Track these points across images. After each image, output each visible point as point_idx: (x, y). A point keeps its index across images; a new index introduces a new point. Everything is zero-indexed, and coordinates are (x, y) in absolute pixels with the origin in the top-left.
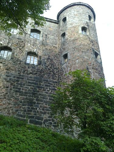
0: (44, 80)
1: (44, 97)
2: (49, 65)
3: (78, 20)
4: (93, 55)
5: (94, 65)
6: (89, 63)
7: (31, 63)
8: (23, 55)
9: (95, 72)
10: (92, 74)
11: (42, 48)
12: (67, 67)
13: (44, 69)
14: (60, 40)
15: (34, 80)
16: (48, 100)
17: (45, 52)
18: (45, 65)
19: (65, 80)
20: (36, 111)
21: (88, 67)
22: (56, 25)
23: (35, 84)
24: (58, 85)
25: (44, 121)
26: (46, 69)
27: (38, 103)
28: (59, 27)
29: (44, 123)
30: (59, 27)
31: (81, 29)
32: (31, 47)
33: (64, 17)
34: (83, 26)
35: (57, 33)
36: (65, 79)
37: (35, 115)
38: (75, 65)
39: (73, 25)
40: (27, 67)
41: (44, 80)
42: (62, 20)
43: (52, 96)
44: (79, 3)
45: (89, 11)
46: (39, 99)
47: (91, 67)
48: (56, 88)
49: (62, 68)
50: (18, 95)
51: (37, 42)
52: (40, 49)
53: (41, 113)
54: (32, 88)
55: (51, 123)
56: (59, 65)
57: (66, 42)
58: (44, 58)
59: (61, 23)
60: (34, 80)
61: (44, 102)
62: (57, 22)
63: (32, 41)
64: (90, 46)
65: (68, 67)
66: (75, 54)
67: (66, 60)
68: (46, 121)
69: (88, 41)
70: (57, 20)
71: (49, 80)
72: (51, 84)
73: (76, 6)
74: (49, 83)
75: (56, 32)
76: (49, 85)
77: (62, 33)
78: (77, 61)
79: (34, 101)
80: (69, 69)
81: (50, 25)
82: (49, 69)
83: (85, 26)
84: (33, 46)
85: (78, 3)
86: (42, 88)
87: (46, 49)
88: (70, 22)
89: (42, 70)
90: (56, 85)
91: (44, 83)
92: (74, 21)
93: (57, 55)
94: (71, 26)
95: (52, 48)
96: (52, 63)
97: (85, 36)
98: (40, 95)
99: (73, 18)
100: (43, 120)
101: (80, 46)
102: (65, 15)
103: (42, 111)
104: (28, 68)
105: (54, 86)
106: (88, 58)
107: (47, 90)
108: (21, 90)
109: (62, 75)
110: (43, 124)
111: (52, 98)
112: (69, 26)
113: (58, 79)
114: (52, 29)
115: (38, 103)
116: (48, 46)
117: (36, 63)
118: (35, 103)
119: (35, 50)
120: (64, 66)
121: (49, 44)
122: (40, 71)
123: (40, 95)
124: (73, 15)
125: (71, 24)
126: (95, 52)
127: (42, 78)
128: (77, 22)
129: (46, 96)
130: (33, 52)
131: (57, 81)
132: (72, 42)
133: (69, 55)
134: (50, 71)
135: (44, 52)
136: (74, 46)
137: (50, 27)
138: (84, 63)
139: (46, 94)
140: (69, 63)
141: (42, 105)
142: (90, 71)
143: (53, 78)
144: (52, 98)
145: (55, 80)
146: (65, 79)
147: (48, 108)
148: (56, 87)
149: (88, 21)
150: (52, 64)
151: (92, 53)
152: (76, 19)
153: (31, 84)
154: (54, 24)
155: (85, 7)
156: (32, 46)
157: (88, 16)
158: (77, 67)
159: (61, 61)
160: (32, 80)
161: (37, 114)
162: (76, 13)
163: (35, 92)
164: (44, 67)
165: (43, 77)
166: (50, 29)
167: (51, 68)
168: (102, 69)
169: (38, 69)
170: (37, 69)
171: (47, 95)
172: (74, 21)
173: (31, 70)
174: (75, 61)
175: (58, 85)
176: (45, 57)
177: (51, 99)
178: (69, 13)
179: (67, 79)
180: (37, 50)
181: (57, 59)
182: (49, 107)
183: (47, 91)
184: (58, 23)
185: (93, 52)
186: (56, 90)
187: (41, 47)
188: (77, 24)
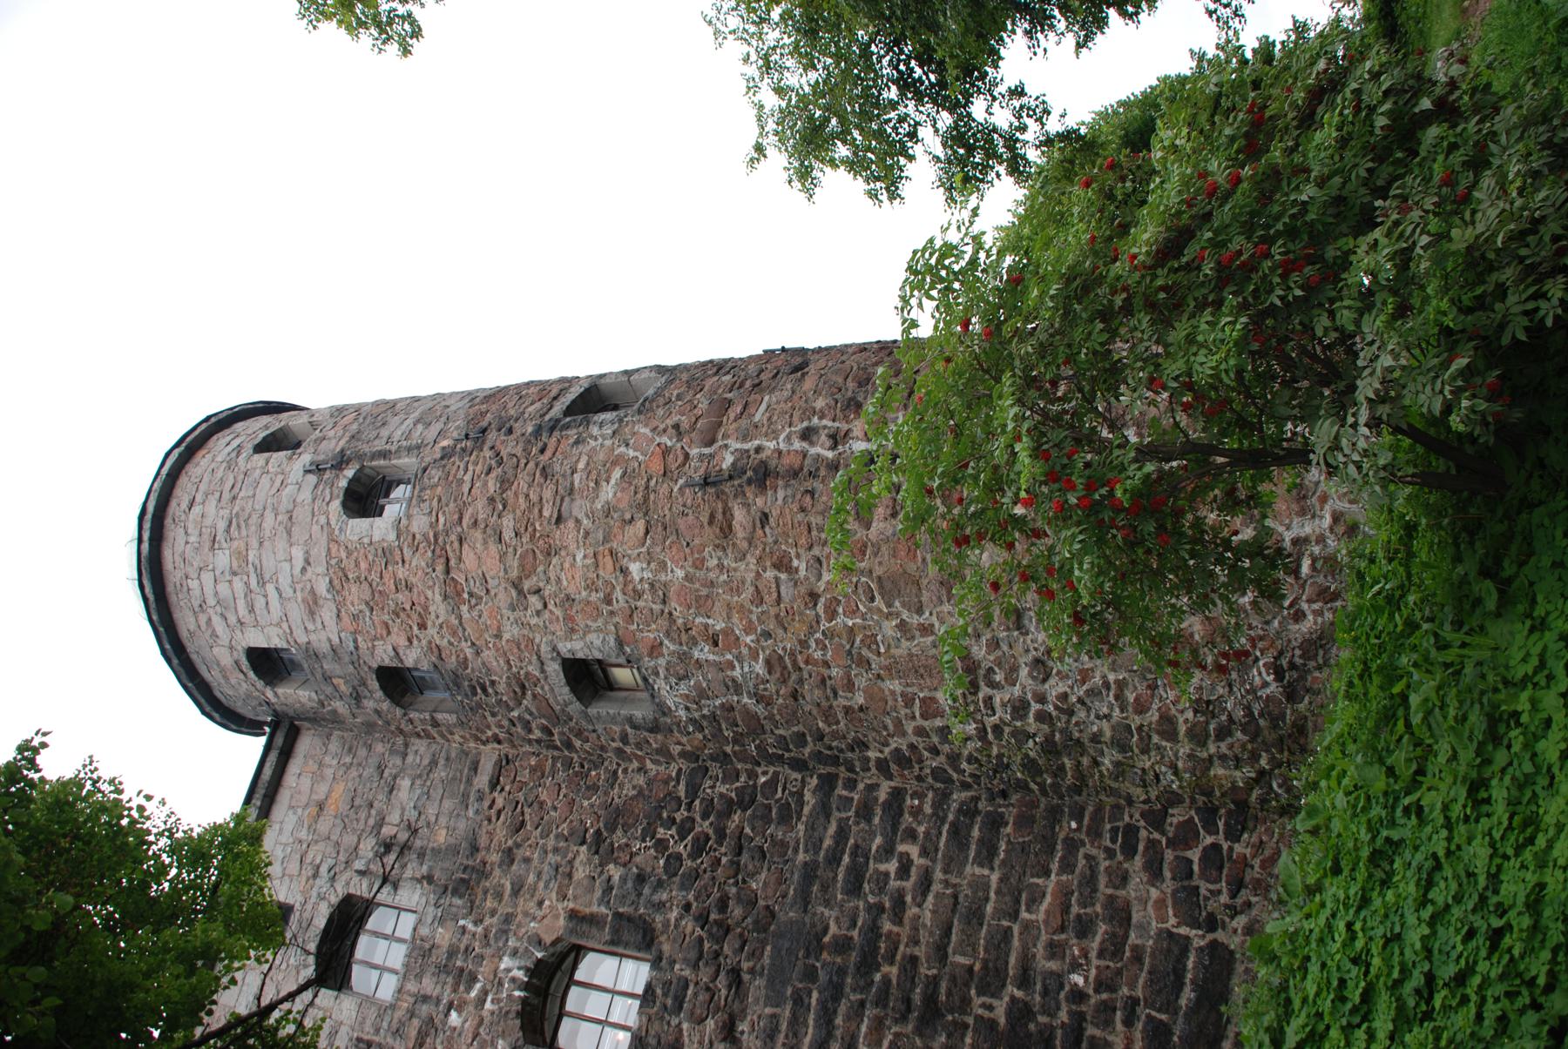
0: (804, 900)
1: (961, 909)
2: (661, 845)
3: (281, 544)
4: (595, 430)
5: (685, 425)
6: (656, 467)
7: (632, 1020)
9: (744, 422)
10: (758, 450)
11: (499, 896)
12: (683, 668)
13: (691, 897)
14: (439, 716)
15: (799, 1001)
16: (995, 878)
17: (539, 875)
18: (660, 884)
19: (811, 693)
20: (1104, 1002)
21: (697, 478)
22: (307, 743)
23: (835, 992)
24: (851, 769)
25: (1195, 924)
26: (696, 875)
27: (1024, 981)
28: (323, 720)
29: (1212, 924)
30: (323, 720)
31: (359, 527)
32: (481, 1001)
33: (245, 663)
34: (336, 504)
35: (379, 748)
36: (795, 695)
37: (1143, 1012)
38: (672, 594)
39: (322, 587)
41: (804, 900)
42: (269, 694)
43: (959, 835)
44: (147, 525)
45: (221, 445)
46: (985, 967)
47: (694, 452)
48: (882, 795)
49: (692, 721)
51: (444, 936)
52: (508, 919)
53: (1114, 947)
54: (878, 1026)
55: (1213, 857)
56: (664, 752)
57: (464, 663)
58: (591, 890)
59: (293, 695)
60: (799, 1001)
61: (1014, 916)
62: (279, 740)
63: (428, 985)
64: (519, 451)
65: (684, 657)
66: (571, 590)
67: (623, 675)
68: (1188, 903)
69: (469, 471)
70: (263, 740)
71: (801, 857)
72: (842, 834)
73: (167, 554)
74: (834, 859)
75: (362, 752)
76: (854, 854)
77: (376, 700)
78: (635, 568)
79: (1000, 1014)
80: (703, 652)
81: (304, 799)
82: (699, 848)
83: (343, 483)
84: (473, 979)
85: (146, 536)
86: (873, 930)
87: (509, 856)
88: (297, 613)
89: (703, 920)
90: (851, 784)
91: (827, 904)
92: (285, 582)
93: (568, 764)
94: (327, 613)
95: (500, 802)
96: (640, 808)
97: (427, 494)
98: (941, 952)
99: (262, 582)
100: (1183, 930)
101: (508, 535)
102: (226, 660)
103: (1098, 938)
105: (865, 812)
106: (617, 473)
107: (894, 884)
109: (756, 727)
110: (1220, 935)
111: (976, 833)
112: (325, 632)
113: (799, 765)
114: (340, 788)
115: (1024, 981)
116: (483, 841)
117: (634, 974)
118: (1020, 1012)
119: (506, 962)
120: (673, 696)
121: (462, 825)
122: (710, 934)
123: (941, 952)
124: (238, 585)
125: (312, 605)
126: (569, 411)
127: (782, 917)
128: (298, 554)
129: (955, 897)
130: (526, 987)
131: (815, 781)
132: (464, 608)
133: (576, 647)
134: (721, 835)
135: (531, 878)
136: (504, 596)
137: (321, 806)
138: (661, 508)
139: (936, 887)
140: (655, 649)
141: (1044, 937)
142: (729, 460)
143: (787, 815)
144: (976, 833)
145: (808, 796)
146: (795, 695)
147: (1073, 880)
148: (873, 788)
149: (305, 458)
150: (654, 819)
151: (572, 432)
152: (269, 565)
153: (830, 1035)
154: (294, 767)
155: (183, 480)
156: (469, 989)
157: (260, 459)
158: (688, 578)
159: (630, 720)
160: (796, 1022)
161: (1125, 991)
162: (223, 559)
163: (917, 997)
164: (673, 894)
165: (773, 915)
166: (330, 810)
168: (719, 367)
169: (693, 955)
170: (695, 967)
171: (946, 883)
172: (285, 582)
173: (702, 1021)
174: (638, 595)
175: (851, 769)
176: (580, 873)
177: (981, 841)
178: (216, 620)
179: (801, 681)
180: (514, 953)
181: (611, 761)
182: (1055, 866)
183: (908, 885)
184: (293, 734)
185: (567, 427)
186: (897, 795)
187: (490, 903)
188: (319, 552)
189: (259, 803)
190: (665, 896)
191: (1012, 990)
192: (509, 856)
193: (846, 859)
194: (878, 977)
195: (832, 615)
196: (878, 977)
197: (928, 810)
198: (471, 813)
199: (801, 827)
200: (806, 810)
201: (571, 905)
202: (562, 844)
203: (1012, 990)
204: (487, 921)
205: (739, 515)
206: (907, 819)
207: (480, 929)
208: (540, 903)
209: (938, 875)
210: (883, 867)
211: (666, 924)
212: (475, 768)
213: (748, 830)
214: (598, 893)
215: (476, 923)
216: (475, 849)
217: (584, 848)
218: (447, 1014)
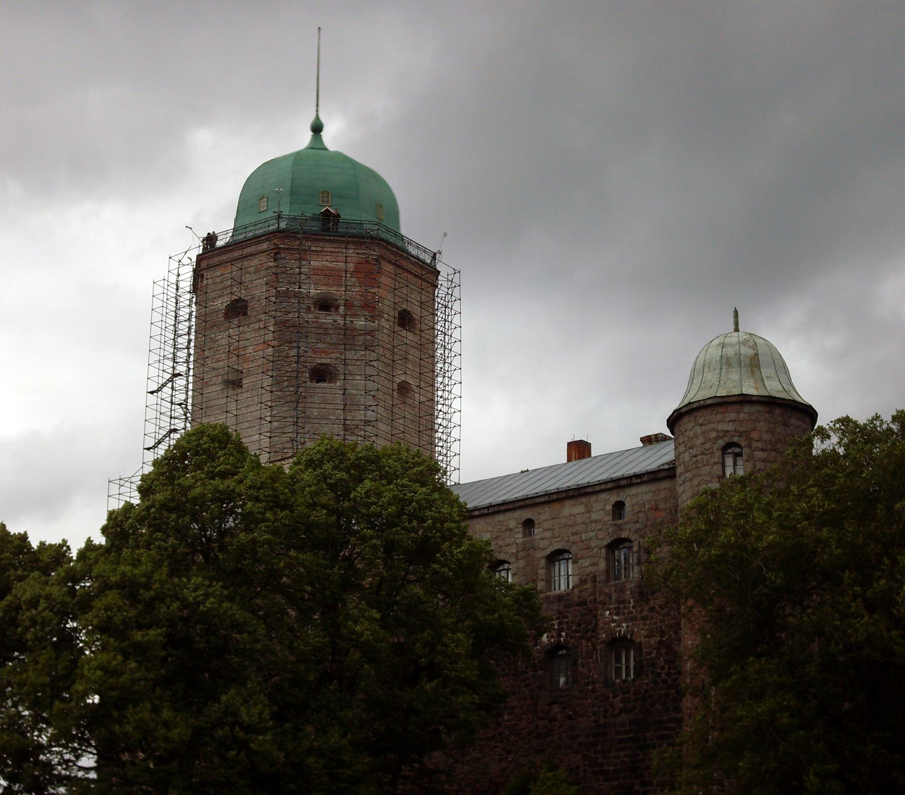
17: (650, 625)
40: (611, 695)
50: (601, 783)
82: (665, 682)
87: (652, 609)
89: (646, 691)
108: (606, 768)
116: (656, 596)
135: (648, 622)
167: (668, 674)
180: (627, 626)
189: (650, 479)
190: (650, 676)
191: (642, 789)
192: (652, 609)
193: (666, 732)
194: (639, 752)
196: (639, 752)
199: (673, 715)
200: (678, 715)
201: (643, 642)
202: (659, 629)
203: (642, 789)
204: (634, 611)
207: (631, 609)
208: (642, 629)
211: (643, 680)
213: (671, 697)
214: (648, 650)
215: (633, 607)
216: (653, 593)
217: (659, 638)
218: (608, 610)
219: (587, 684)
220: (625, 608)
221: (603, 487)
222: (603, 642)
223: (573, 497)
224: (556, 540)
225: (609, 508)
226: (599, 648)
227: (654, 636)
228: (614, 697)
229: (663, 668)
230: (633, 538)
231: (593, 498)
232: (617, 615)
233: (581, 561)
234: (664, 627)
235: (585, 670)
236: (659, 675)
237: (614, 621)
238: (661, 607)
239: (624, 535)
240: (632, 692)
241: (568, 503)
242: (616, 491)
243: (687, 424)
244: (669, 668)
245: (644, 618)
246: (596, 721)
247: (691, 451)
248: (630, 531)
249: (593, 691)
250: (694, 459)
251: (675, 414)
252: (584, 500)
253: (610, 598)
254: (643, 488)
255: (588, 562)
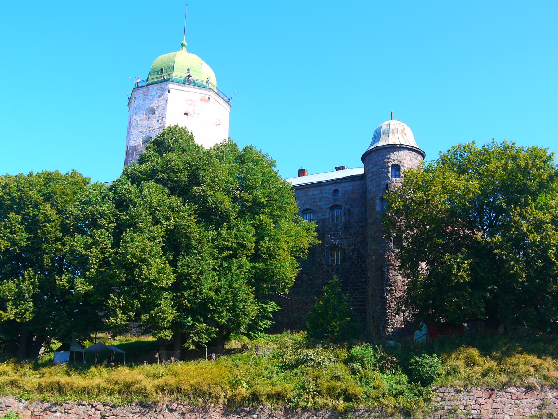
8: (324, 254)
17: (349, 241)
40: (331, 271)
82: (356, 265)
87: (351, 235)
101: (377, 234)
104: (332, 271)
106: (383, 252)
107: (354, 294)
111: (361, 303)
135: (348, 240)
139: (354, 300)
142: (384, 269)
144: (361, 303)
167: (358, 262)
176: (350, 248)
180: (339, 241)
195: (371, 286)
197: (364, 297)
198: (356, 224)
205: (378, 272)
206: (362, 294)
208: (346, 243)
209: (356, 300)
210: (356, 293)
211: (346, 264)
212: (362, 221)
214: (348, 252)
219: (320, 266)
220: (338, 234)
221: (329, 183)
222: (328, 248)
223: (315, 187)
224: (306, 204)
225: (331, 192)
226: (325, 250)
227: (351, 246)
228: (332, 271)
229: (355, 260)
230: (342, 205)
231: (324, 187)
232: (334, 236)
233: (318, 214)
234: (356, 242)
235: (318, 260)
236: (353, 262)
237: (332, 239)
238: (355, 234)
239: (338, 203)
240: (341, 270)
241: (312, 189)
242: (335, 185)
243: (367, 158)
244: (358, 260)
245: (347, 238)
246: (323, 281)
247: (376, 167)
248: (341, 202)
249: (322, 268)
250: (378, 170)
251: (368, 152)
252: (319, 188)
253: (331, 229)
254: (347, 184)
255: (321, 214)
